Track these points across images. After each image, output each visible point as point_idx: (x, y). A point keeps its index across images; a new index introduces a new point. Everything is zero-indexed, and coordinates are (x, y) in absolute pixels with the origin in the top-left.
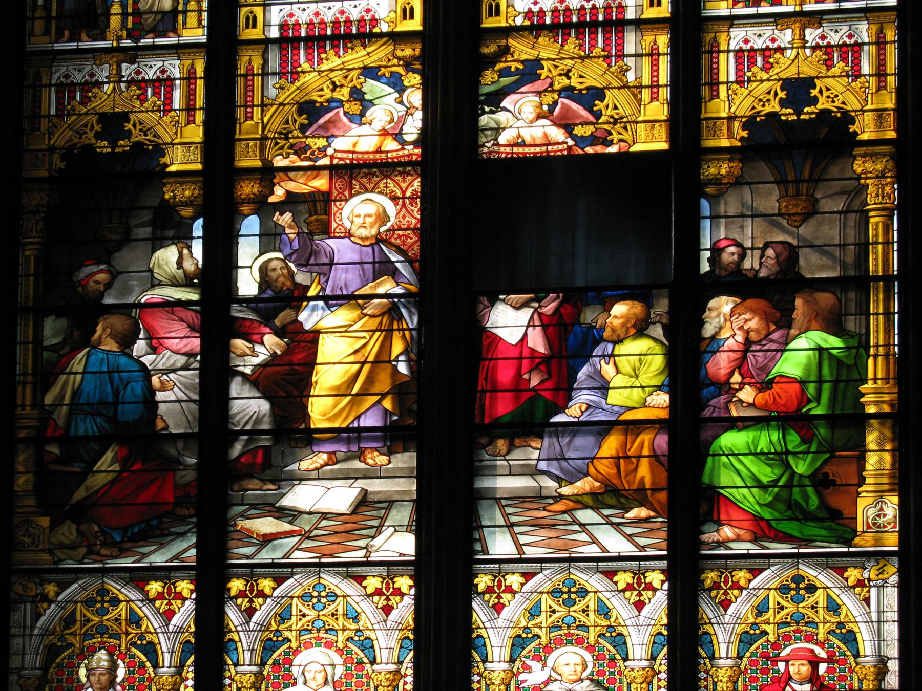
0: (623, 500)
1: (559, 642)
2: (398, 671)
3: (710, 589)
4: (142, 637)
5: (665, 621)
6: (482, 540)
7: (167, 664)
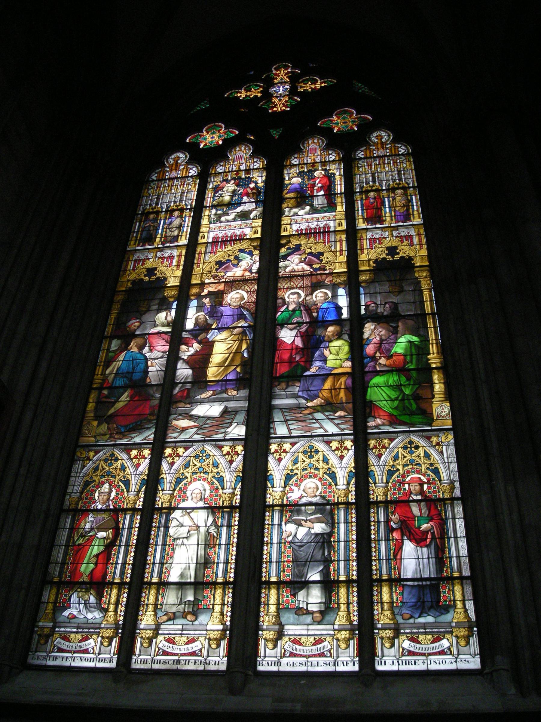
0: (334, 408)
1: (306, 477)
2: (233, 493)
3: (372, 449)
4: (125, 477)
5: (353, 465)
6: (274, 428)
7: (133, 490)
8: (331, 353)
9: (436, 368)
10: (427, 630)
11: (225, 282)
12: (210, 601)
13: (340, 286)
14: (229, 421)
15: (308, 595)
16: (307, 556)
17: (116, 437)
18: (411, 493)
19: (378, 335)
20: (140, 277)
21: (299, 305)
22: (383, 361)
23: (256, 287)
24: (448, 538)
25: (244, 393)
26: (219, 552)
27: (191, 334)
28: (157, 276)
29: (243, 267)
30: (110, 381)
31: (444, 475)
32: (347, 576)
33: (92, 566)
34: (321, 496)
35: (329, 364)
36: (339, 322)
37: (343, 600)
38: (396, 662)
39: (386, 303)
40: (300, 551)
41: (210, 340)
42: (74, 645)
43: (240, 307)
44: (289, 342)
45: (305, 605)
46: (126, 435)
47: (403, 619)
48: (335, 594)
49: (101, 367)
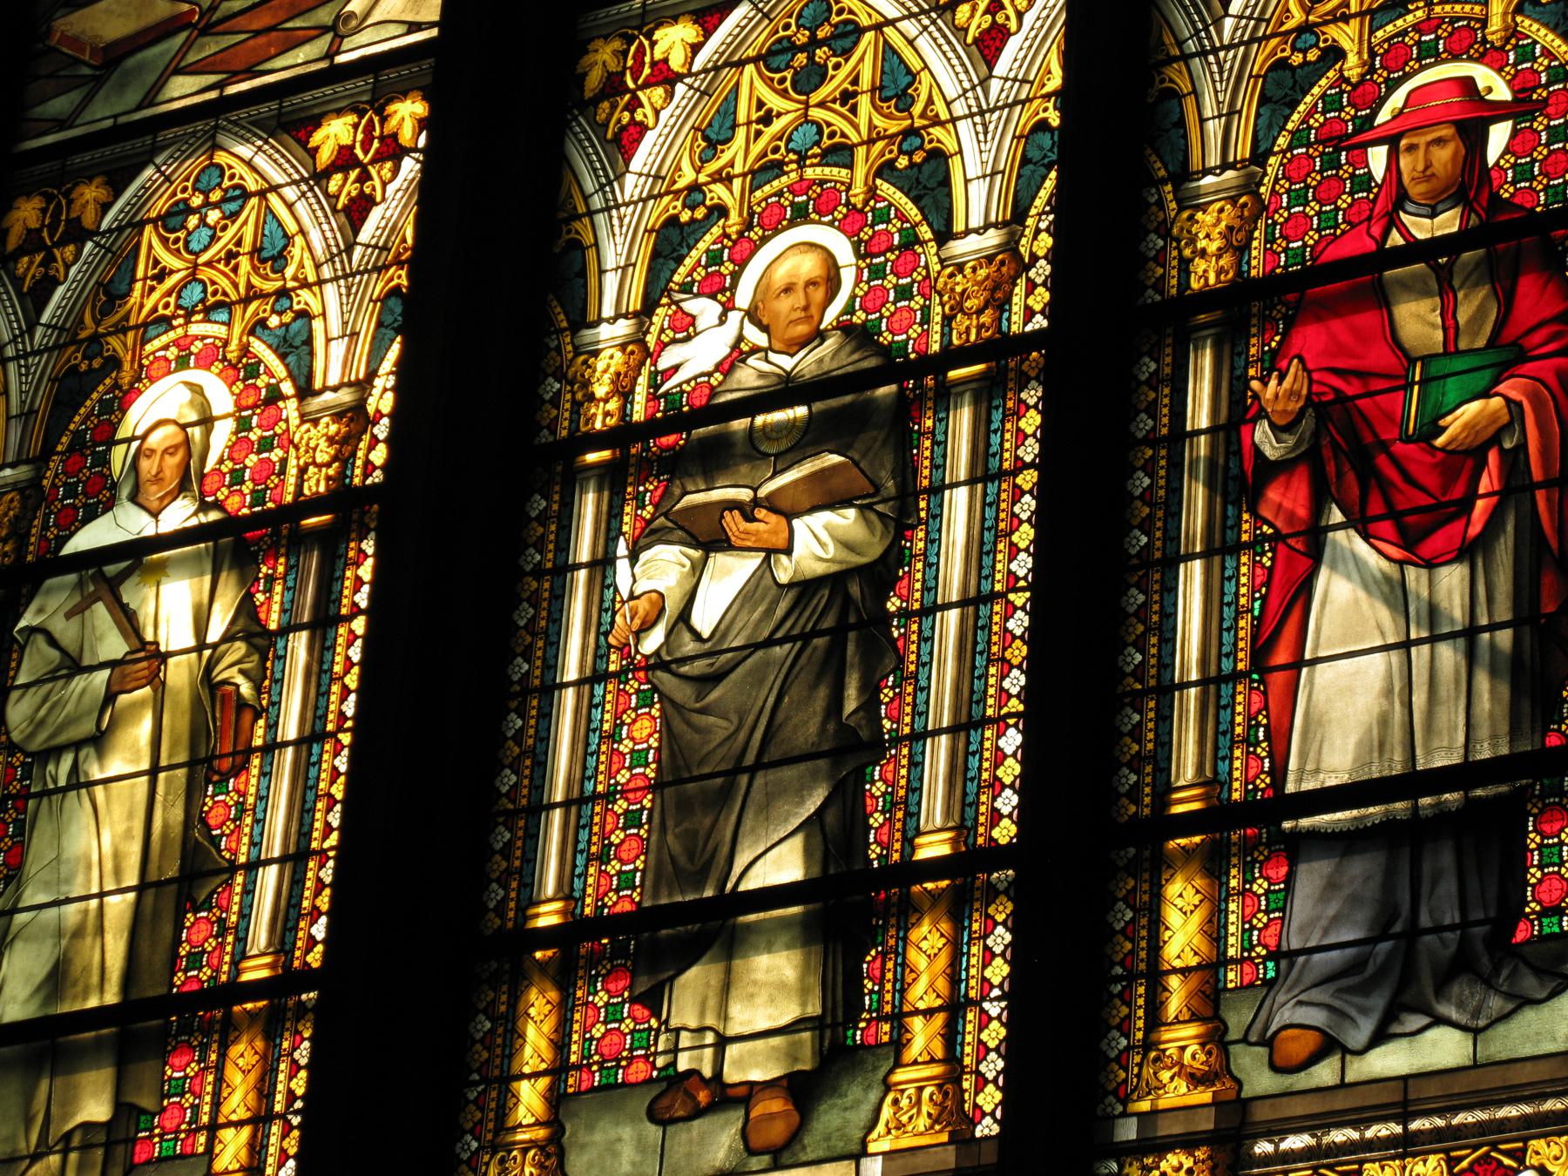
2: (359, 408)
10: (1415, 1125)
12: (196, 1109)
16: (742, 736)
18: (1401, 198)
26: (262, 798)
32: (963, 829)
40: (703, 711)
45: (708, 1053)
47: (1275, 1068)
48: (884, 956)
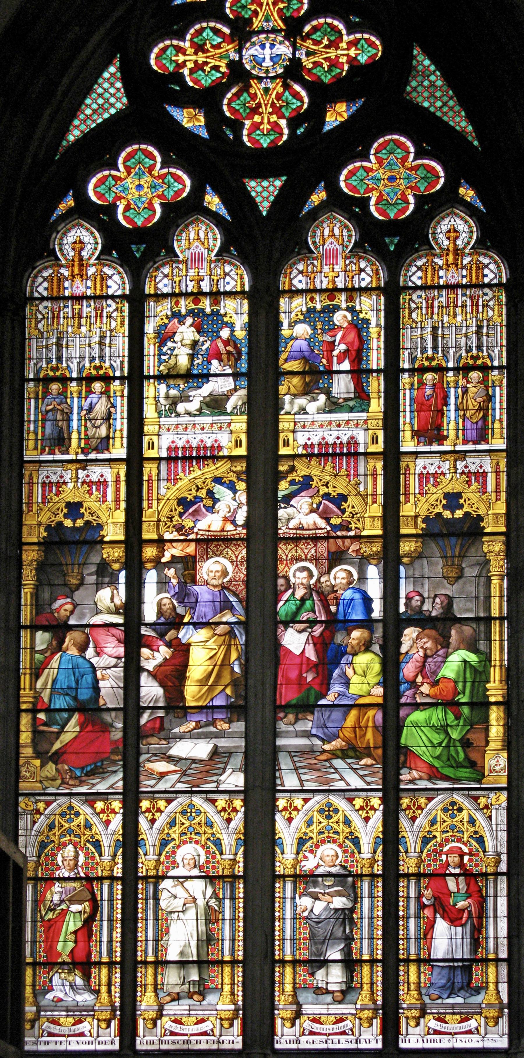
1: (323, 842)
2: (234, 860)
3: (405, 810)
4: (92, 837)
5: (381, 829)
6: (281, 778)
8: (355, 673)
9: (496, 703)
11: (197, 541)
13: (372, 561)
14: (222, 766)
15: (327, 974)
17: (71, 782)
18: (449, 865)
19: (422, 647)
20: (58, 519)
21: (310, 589)
22: (425, 689)
23: (244, 552)
24: (487, 917)
25: (240, 726)
26: (223, 928)
27: (154, 630)
28: (85, 519)
29: (222, 514)
30: (46, 700)
31: (490, 846)
32: (371, 955)
33: (71, 945)
34: (341, 866)
35: (354, 689)
36: (367, 623)
37: (366, 979)
38: (420, 1040)
39: (436, 596)
41: (184, 642)
42: (67, 1029)
43: (224, 587)
44: (298, 652)
46: (84, 781)
49: (28, 677)
